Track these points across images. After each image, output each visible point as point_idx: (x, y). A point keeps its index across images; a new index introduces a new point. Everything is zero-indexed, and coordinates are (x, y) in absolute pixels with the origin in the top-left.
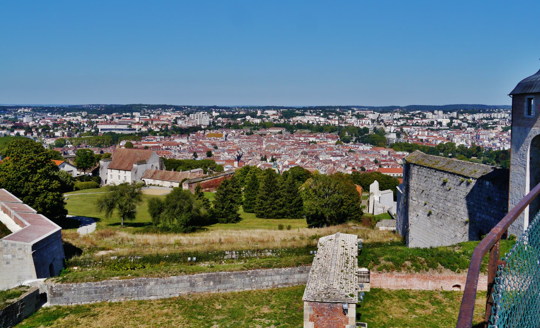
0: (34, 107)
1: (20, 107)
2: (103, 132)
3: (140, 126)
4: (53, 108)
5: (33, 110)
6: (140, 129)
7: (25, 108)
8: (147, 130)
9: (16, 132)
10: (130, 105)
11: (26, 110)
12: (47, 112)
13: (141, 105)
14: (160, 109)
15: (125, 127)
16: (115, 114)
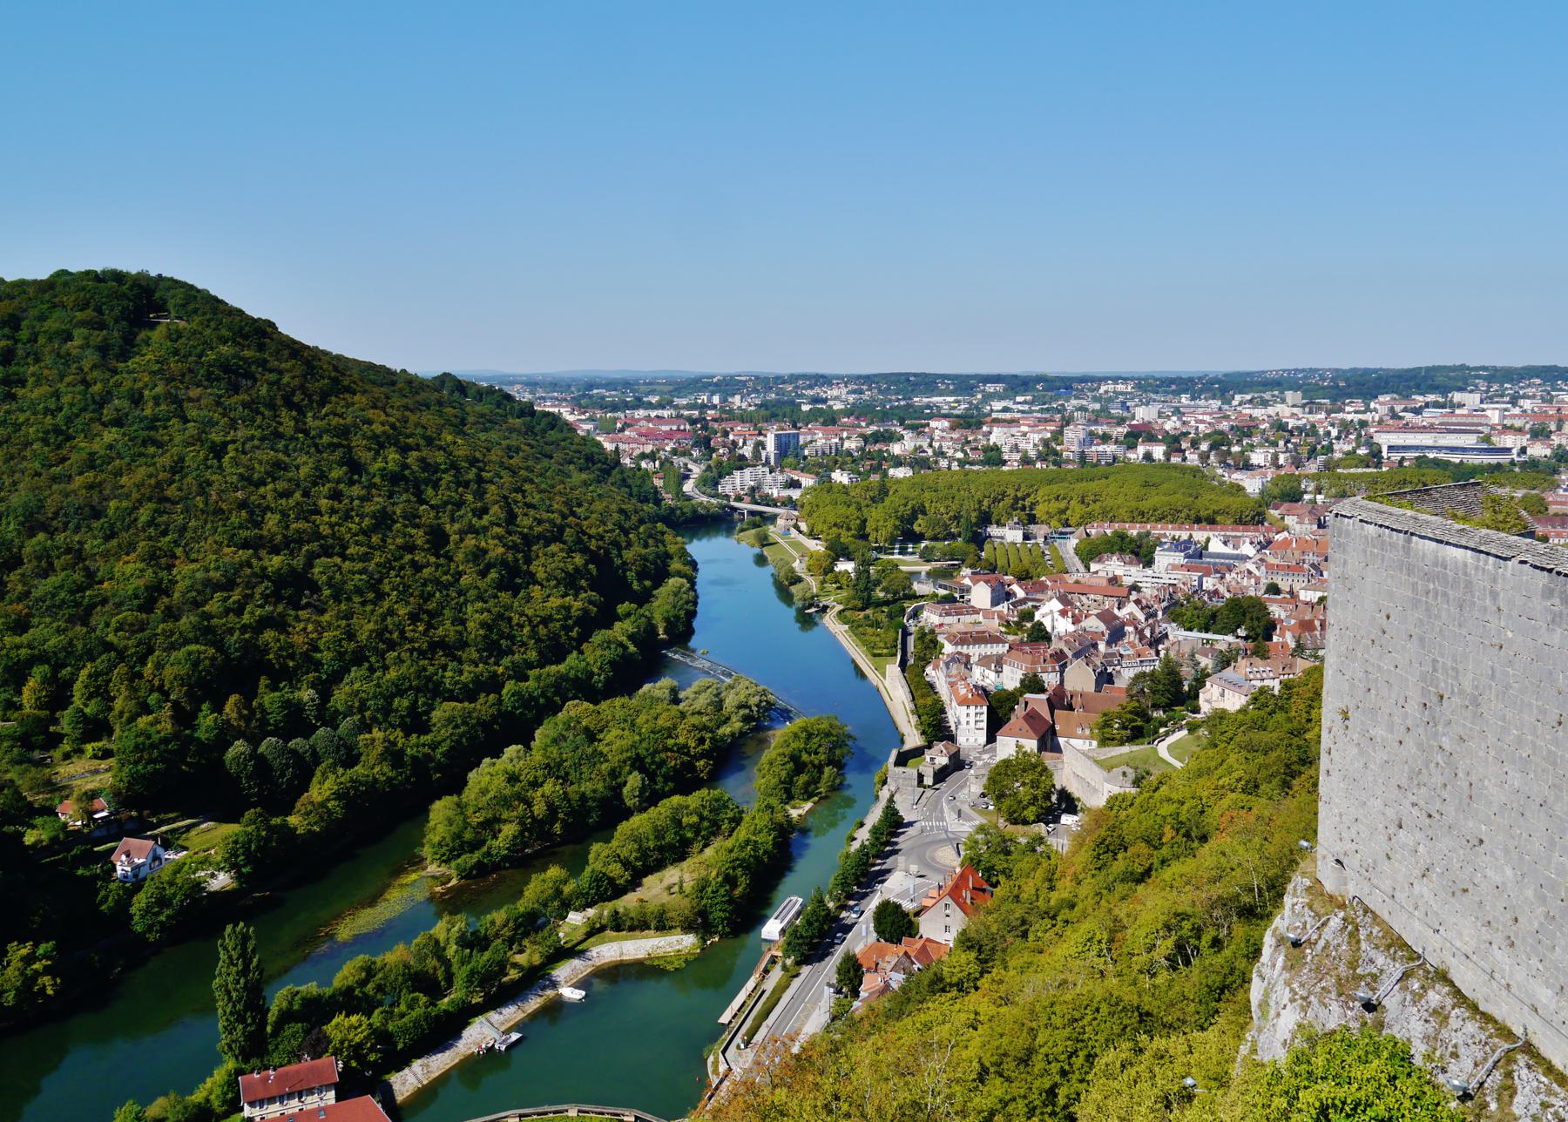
0: (1140, 379)
1: (1105, 379)
2: (1396, 457)
3: (1523, 440)
4: (1191, 380)
5: (1138, 386)
6: (1523, 450)
7: (1115, 380)
8: (1548, 452)
9: (1141, 450)
10: (1428, 369)
11: (1120, 388)
12: (1177, 393)
13: (1463, 367)
14: (1538, 381)
15: (1470, 440)
16: (1387, 398)
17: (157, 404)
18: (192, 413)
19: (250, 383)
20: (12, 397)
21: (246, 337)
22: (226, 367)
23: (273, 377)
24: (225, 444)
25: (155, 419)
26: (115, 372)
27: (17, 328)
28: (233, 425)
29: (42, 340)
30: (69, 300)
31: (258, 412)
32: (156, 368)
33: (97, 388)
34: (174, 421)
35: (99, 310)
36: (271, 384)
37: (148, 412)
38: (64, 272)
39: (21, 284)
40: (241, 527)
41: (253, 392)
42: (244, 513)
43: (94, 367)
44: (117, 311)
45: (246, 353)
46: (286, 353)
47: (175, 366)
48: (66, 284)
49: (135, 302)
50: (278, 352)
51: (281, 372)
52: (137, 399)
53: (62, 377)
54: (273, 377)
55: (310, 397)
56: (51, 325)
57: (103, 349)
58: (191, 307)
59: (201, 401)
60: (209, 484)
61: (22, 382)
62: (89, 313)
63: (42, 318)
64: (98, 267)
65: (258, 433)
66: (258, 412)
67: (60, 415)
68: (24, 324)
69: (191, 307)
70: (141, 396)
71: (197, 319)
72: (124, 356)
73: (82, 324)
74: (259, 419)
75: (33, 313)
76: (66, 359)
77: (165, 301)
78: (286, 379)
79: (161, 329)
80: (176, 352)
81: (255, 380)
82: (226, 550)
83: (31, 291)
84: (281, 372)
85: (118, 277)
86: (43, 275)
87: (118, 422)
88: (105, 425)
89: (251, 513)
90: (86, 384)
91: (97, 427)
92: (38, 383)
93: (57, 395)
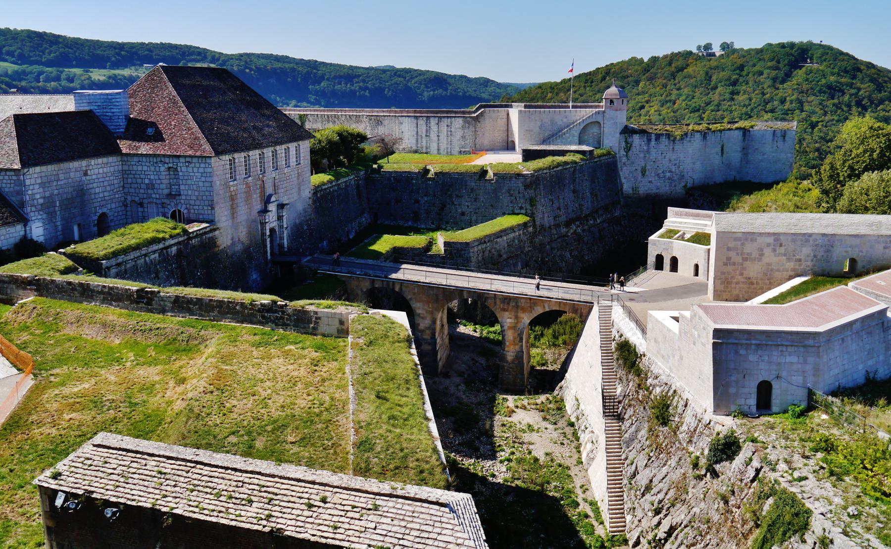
17: (791, 103)
18: (806, 107)
19: (840, 94)
20: (733, 99)
21: (846, 71)
22: (830, 87)
23: (853, 91)
24: (818, 122)
25: (789, 110)
26: (778, 89)
27: (742, 70)
28: (825, 114)
29: (750, 75)
30: (766, 57)
31: (840, 108)
32: (795, 87)
33: (768, 96)
34: (797, 111)
35: (778, 62)
36: (851, 95)
37: (786, 107)
38: (770, 45)
39: (750, 50)
40: (813, 159)
41: (841, 99)
42: (816, 154)
43: (769, 86)
44: (786, 62)
45: (843, 80)
46: (867, 79)
47: (805, 87)
48: (767, 50)
49: (795, 56)
50: (863, 78)
51: (859, 89)
52: (783, 101)
53: (754, 91)
54: (853, 91)
55: (872, 102)
56: (757, 68)
57: (774, 80)
58: (824, 58)
59: (813, 103)
60: (804, 139)
61: (738, 93)
62: (774, 63)
63: (754, 65)
64: (785, 40)
65: (836, 118)
66: (840, 108)
67: (749, 108)
68: (745, 69)
69: (824, 58)
70: (785, 100)
71: (825, 63)
72: (783, 82)
73: (769, 68)
74: (839, 111)
75: (751, 63)
76: (758, 83)
77: (813, 55)
78: (860, 93)
79: (804, 69)
80: (807, 80)
81: (844, 93)
82: (803, 168)
83: (752, 53)
84: (859, 89)
85: (792, 45)
86: (759, 46)
87: (772, 111)
88: (766, 112)
89: (820, 154)
90: (763, 94)
91: (763, 112)
92: (744, 93)
93: (750, 100)
